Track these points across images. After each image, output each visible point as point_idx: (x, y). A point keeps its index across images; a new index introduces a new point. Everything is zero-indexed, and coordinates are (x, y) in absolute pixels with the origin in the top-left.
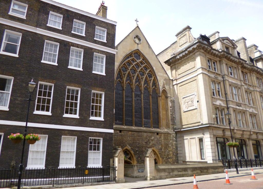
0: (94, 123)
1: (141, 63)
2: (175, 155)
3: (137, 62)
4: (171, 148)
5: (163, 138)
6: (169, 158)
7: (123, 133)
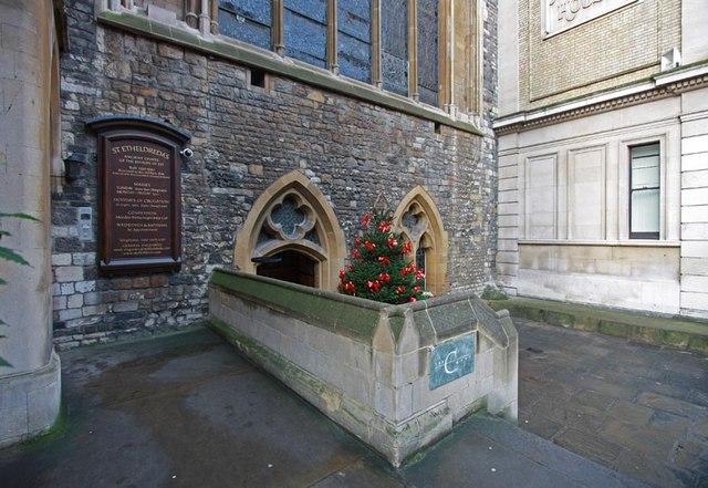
7: (273, 93)
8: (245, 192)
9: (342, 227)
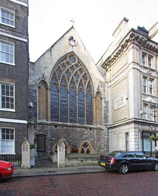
1: (76, 65)
6: (101, 149)
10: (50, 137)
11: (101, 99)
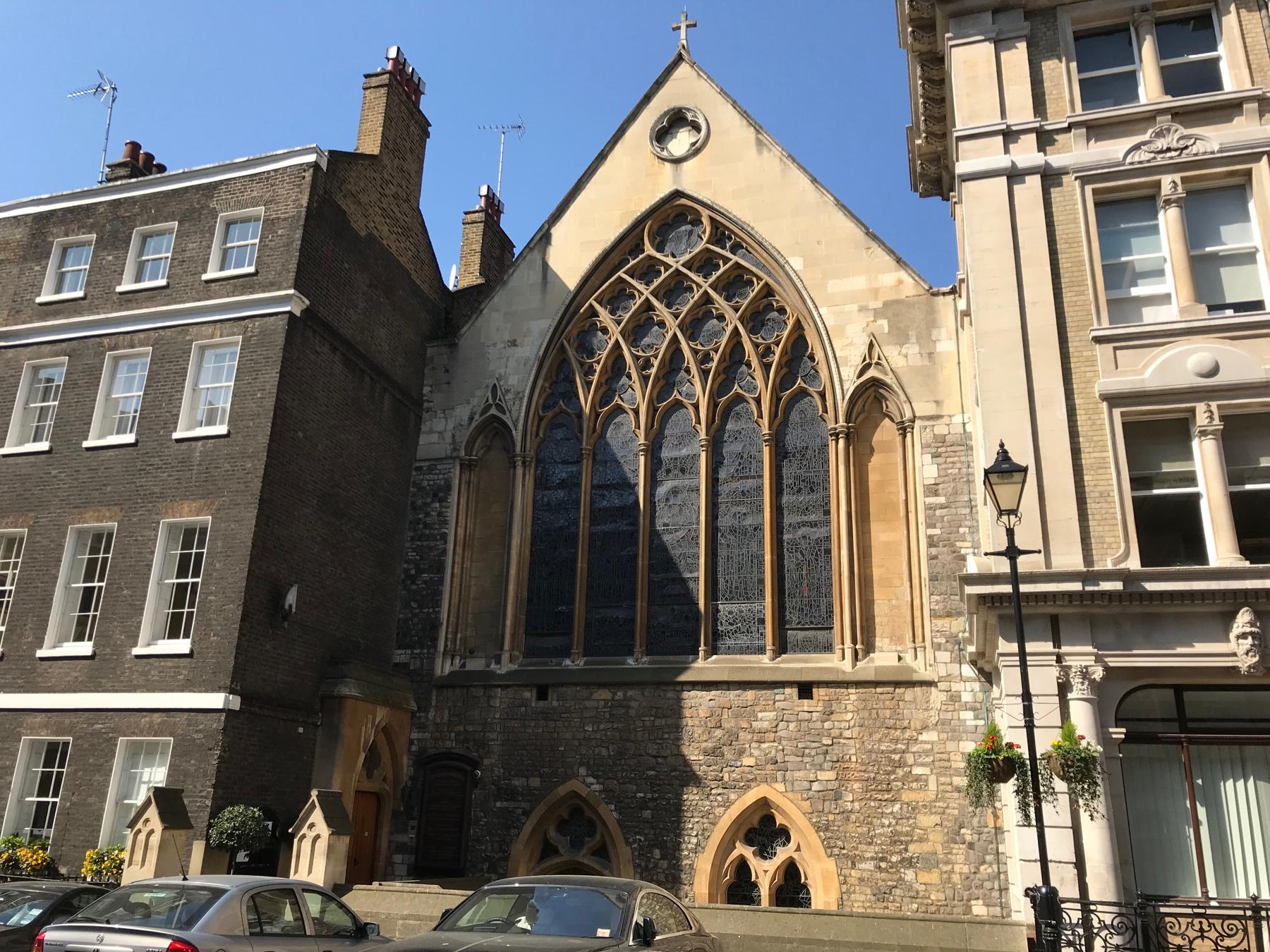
0: (149, 671)
2: (968, 838)
3: (671, 271)
4: (932, 785)
5: (850, 716)
6: (909, 863)
7: (555, 703)
8: (523, 804)
9: (628, 843)
10: (499, 771)
11: (904, 429)
